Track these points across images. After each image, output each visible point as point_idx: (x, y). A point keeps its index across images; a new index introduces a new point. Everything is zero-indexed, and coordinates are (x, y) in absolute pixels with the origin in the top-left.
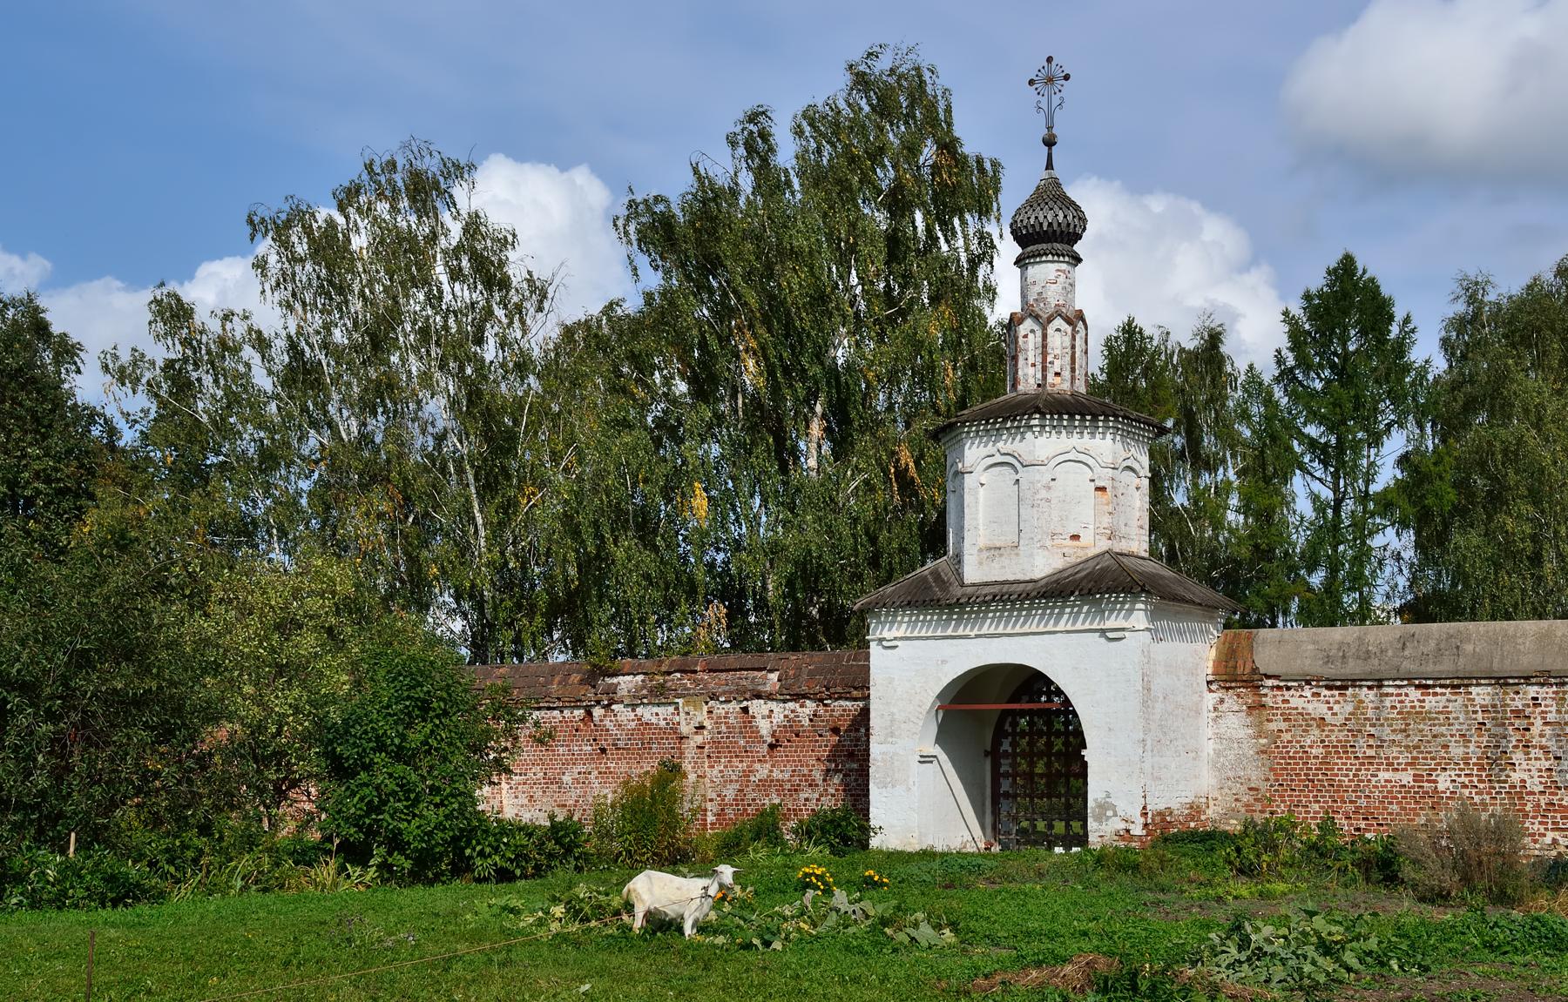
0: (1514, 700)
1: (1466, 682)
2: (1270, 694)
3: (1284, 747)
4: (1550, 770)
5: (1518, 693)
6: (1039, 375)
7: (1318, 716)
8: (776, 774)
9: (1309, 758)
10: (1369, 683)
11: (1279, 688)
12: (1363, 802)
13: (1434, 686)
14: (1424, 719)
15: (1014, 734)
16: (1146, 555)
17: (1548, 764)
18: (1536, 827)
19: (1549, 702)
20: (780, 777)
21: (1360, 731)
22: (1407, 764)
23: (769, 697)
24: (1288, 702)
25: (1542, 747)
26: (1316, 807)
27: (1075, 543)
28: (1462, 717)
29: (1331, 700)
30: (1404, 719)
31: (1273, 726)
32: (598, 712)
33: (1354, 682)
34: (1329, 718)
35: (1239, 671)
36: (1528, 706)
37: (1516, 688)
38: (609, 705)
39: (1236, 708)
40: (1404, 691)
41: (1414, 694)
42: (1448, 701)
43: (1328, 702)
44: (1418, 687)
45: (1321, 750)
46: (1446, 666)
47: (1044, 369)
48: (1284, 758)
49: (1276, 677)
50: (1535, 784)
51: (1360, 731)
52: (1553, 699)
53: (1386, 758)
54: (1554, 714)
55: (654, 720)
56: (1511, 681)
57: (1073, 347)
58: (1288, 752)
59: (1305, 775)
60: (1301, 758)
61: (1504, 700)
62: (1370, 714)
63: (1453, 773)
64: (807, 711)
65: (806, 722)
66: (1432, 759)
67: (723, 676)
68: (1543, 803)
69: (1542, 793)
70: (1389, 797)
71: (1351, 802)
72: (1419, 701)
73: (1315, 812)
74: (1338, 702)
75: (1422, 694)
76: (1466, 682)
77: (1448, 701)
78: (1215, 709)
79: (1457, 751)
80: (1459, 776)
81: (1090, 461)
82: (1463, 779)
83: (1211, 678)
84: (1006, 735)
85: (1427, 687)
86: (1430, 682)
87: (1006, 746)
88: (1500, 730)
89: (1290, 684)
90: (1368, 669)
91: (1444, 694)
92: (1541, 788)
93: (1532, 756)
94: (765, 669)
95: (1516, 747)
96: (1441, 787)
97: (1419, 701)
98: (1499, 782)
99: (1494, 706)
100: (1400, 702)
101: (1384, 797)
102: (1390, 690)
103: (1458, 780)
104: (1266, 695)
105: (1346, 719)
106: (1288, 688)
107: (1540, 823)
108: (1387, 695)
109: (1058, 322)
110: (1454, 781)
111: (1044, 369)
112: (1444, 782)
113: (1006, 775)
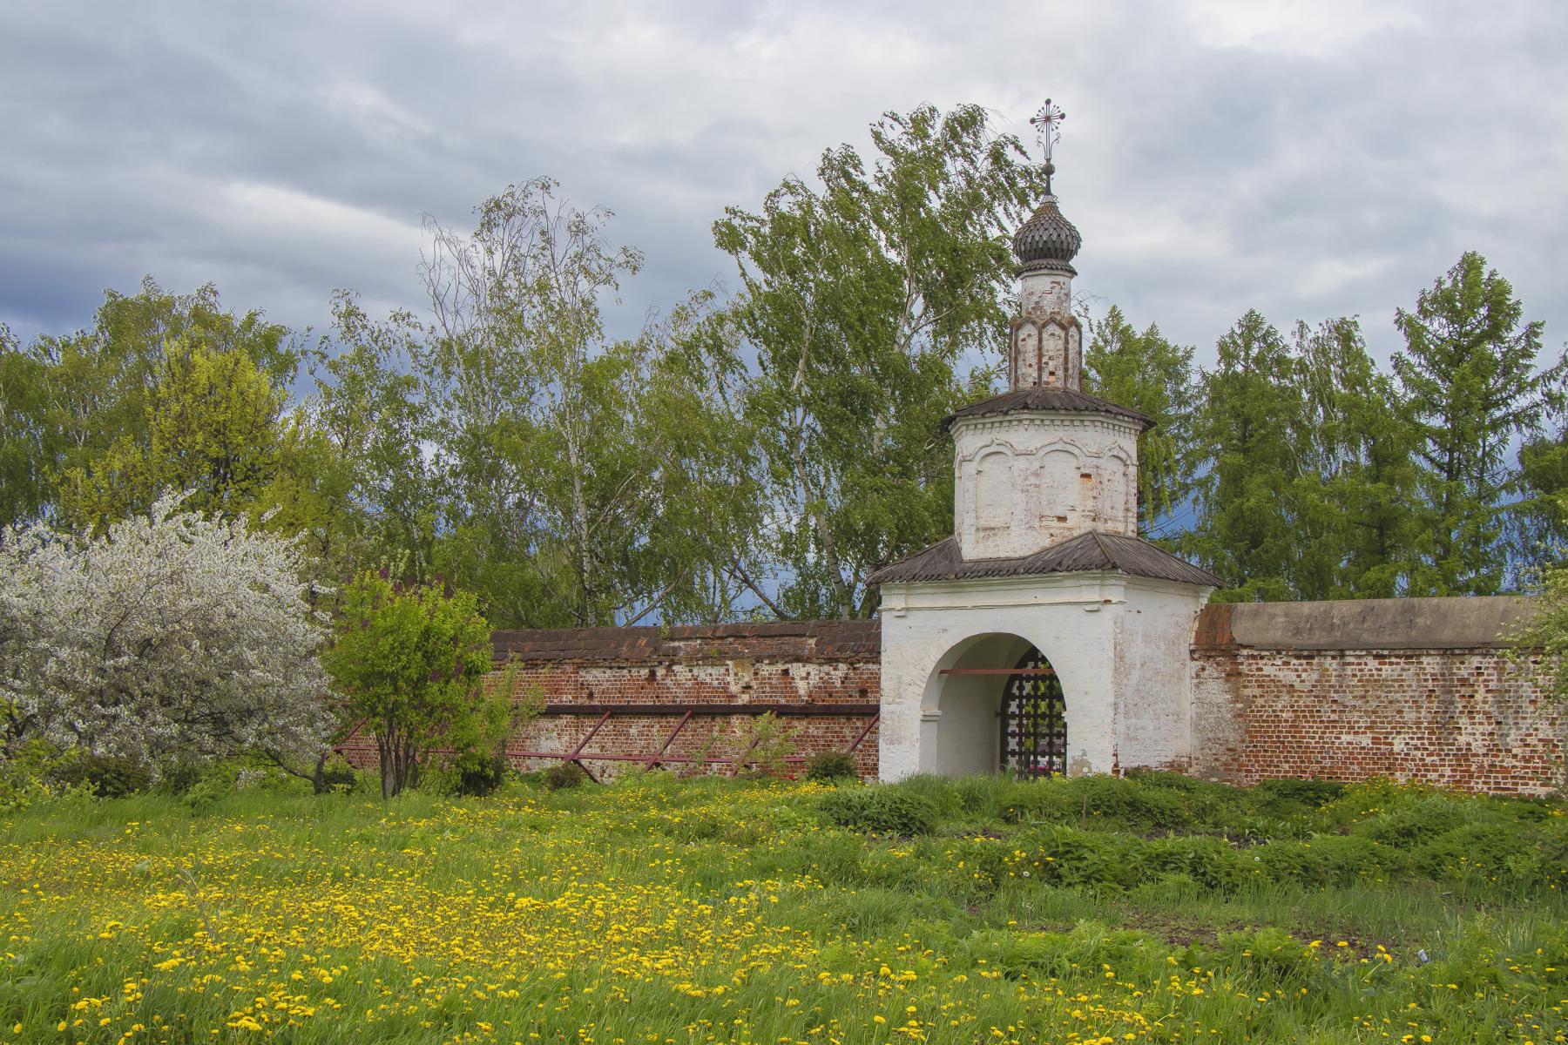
0: (1459, 669)
1: (1417, 652)
4: (1491, 734)
5: (1462, 663)
6: (1035, 374)
7: (1288, 683)
8: (812, 730)
9: (1280, 721)
10: (1332, 653)
11: (1253, 657)
12: (1327, 763)
13: (1390, 656)
14: (1381, 686)
15: (1021, 697)
16: (1135, 535)
17: (1490, 728)
18: (1480, 786)
19: (1491, 671)
20: (815, 733)
21: (1325, 697)
22: (1366, 728)
23: (805, 660)
24: (1261, 669)
25: (1484, 713)
26: (1286, 766)
27: (1062, 524)
28: (1414, 684)
30: (1363, 686)
31: (1248, 692)
32: (660, 672)
33: (1319, 651)
34: (1298, 685)
35: (1218, 641)
36: (1472, 674)
37: (1462, 659)
38: (670, 666)
39: (1215, 675)
40: (1363, 661)
41: (1373, 664)
42: (1403, 669)
43: (1297, 670)
44: (1376, 657)
45: (1291, 714)
46: (1398, 638)
48: (1258, 721)
50: (1478, 746)
51: (1325, 697)
52: (1494, 668)
53: (1349, 722)
54: (1495, 683)
55: (708, 680)
56: (1457, 652)
57: (1066, 349)
59: (1278, 737)
60: (1273, 722)
61: (1451, 669)
62: (1333, 681)
63: (1407, 736)
64: (839, 673)
65: (838, 684)
66: (1389, 723)
67: (769, 641)
68: (1486, 764)
69: (1484, 755)
70: (1350, 758)
71: (1317, 762)
72: (1377, 669)
73: (1286, 772)
74: (1305, 670)
75: (1380, 664)
76: (1417, 652)
77: (1403, 669)
78: (1198, 676)
79: (1410, 716)
80: (1412, 739)
81: (1076, 451)
82: (1415, 741)
83: (1192, 647)
84: (1013, 697)
85: (1384, 657)
86: (1386, 652)
87: (1013, 707)
88: (1448, 697)
89: (1263, 653)
90: (1331, 639)
91: (1398, 664)
92: (1484, 750)
93: (1476, 720)
94: (804, 635)
95: (1461, 712)
96: (1396, 749)
97: (1377, 669)
98: (1448, 744)
99: (1443, 675)
100: (1361, 670)
101: (1347, 758)
102: (1351, 660)
103: (1411, 742)
104: (1242, 664)
105: (1313, 686)
106: (1262, 658)
107: (1484, 783)
108: (1349, 664)
109: (1052, 328)
110: (1407, 744)
111: (1040, 369)
112: (1398, 745)
113: (1013, 735)
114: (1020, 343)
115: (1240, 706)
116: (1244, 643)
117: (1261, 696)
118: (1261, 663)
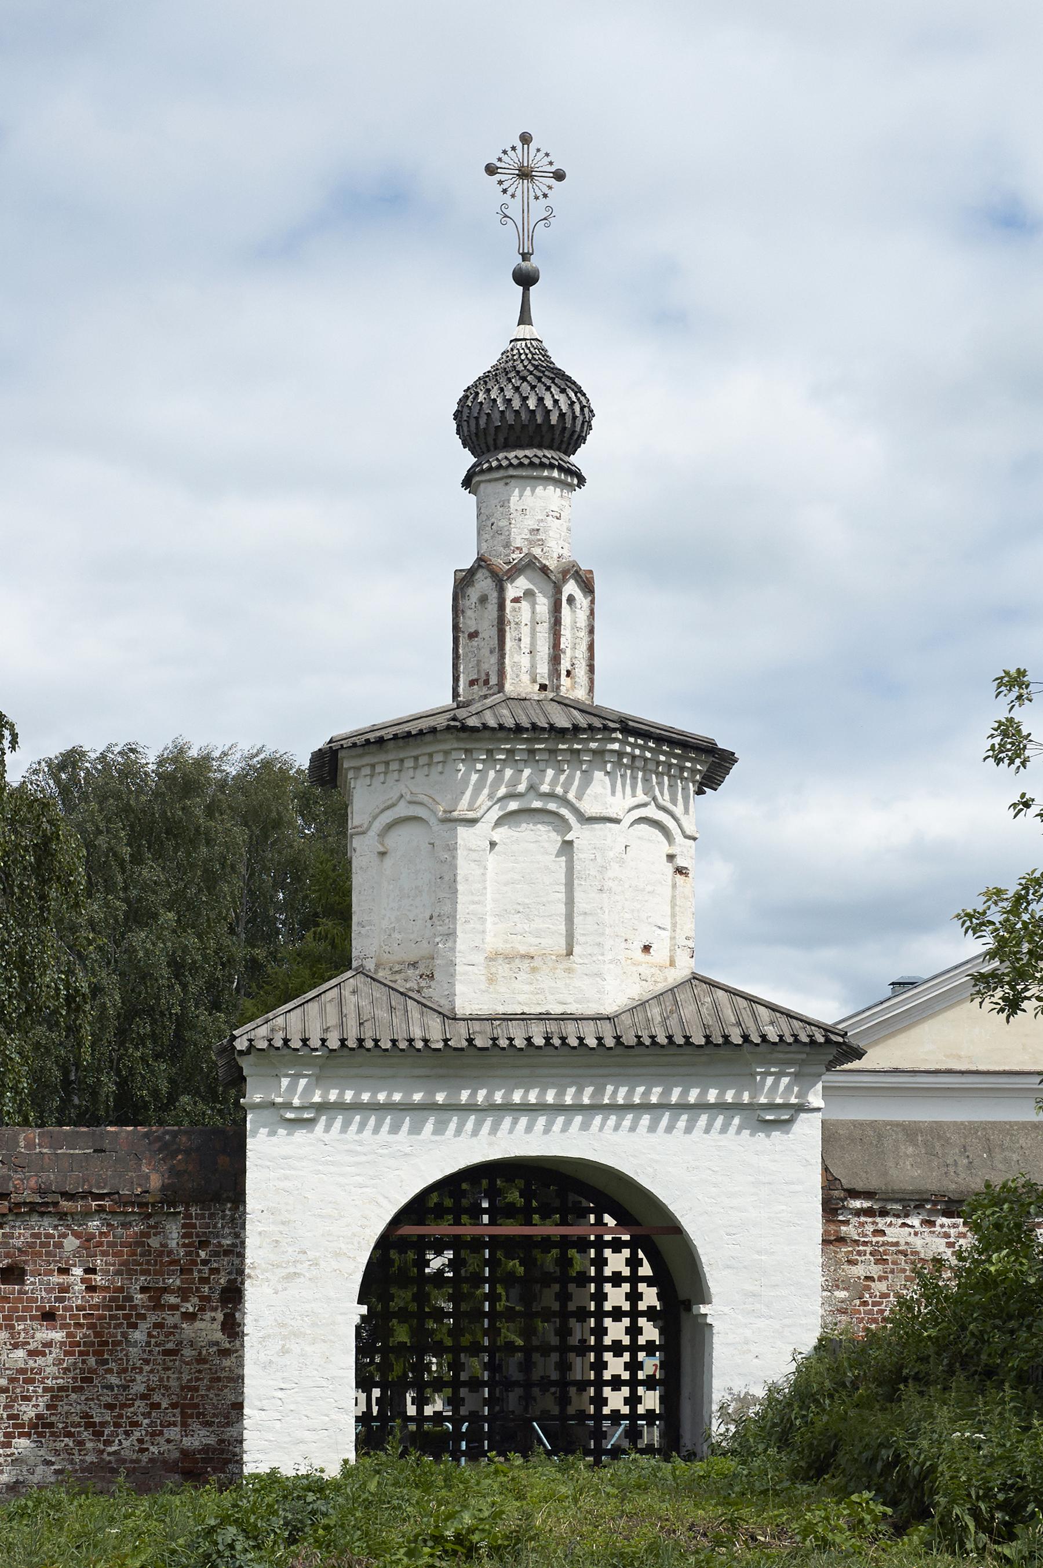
2: (854, 1220)
3: (874, 1304)
7: (930, 1256)
24: (882, 1233)
29: (953, 1232)
43: (947, 1235)
47: (555, 659)
49: (868, 1195)
58: (882, 1311)
81: (671, 824)
104: (846, 1223)
106: (884, 1213)
111: (555, 659)
114: (509, 605)
115: (842, 1294)
116: (859, 1186)
117: (880, 1279)
118: (881, 1222)
